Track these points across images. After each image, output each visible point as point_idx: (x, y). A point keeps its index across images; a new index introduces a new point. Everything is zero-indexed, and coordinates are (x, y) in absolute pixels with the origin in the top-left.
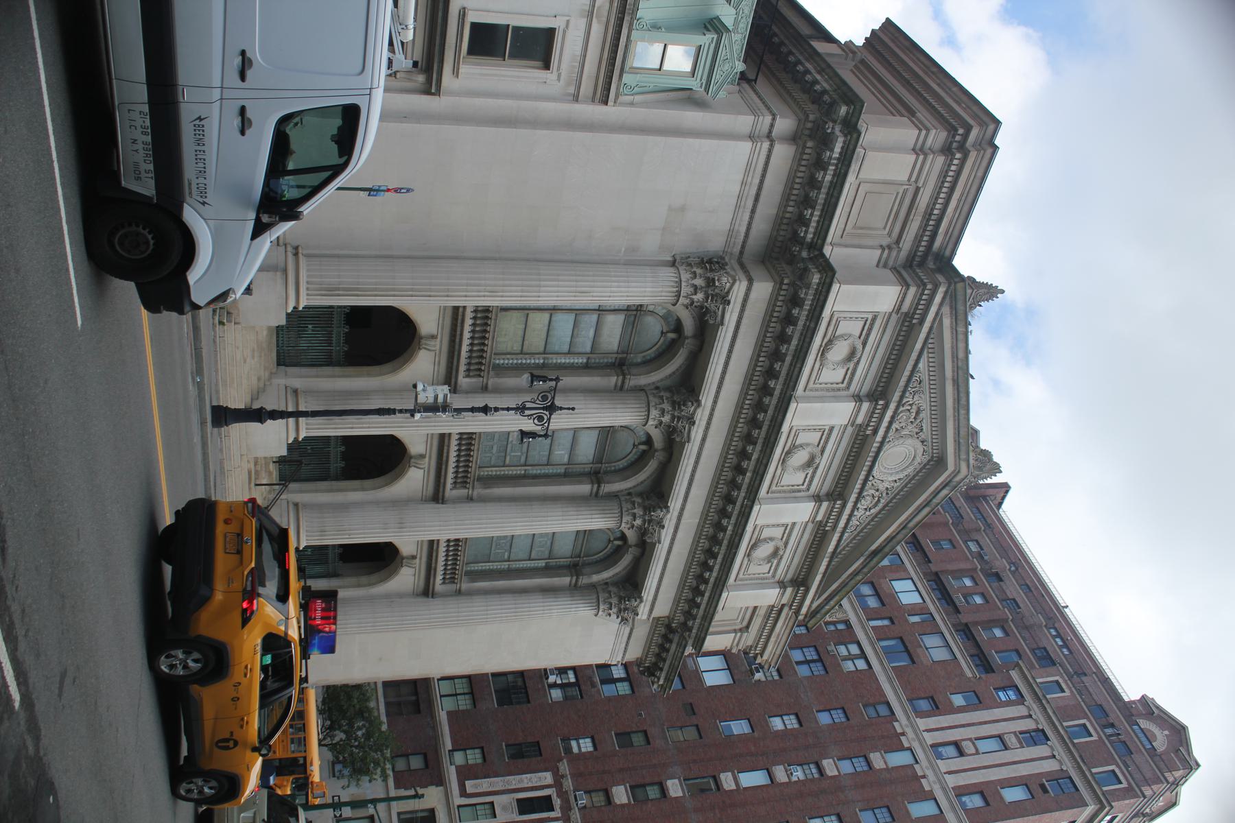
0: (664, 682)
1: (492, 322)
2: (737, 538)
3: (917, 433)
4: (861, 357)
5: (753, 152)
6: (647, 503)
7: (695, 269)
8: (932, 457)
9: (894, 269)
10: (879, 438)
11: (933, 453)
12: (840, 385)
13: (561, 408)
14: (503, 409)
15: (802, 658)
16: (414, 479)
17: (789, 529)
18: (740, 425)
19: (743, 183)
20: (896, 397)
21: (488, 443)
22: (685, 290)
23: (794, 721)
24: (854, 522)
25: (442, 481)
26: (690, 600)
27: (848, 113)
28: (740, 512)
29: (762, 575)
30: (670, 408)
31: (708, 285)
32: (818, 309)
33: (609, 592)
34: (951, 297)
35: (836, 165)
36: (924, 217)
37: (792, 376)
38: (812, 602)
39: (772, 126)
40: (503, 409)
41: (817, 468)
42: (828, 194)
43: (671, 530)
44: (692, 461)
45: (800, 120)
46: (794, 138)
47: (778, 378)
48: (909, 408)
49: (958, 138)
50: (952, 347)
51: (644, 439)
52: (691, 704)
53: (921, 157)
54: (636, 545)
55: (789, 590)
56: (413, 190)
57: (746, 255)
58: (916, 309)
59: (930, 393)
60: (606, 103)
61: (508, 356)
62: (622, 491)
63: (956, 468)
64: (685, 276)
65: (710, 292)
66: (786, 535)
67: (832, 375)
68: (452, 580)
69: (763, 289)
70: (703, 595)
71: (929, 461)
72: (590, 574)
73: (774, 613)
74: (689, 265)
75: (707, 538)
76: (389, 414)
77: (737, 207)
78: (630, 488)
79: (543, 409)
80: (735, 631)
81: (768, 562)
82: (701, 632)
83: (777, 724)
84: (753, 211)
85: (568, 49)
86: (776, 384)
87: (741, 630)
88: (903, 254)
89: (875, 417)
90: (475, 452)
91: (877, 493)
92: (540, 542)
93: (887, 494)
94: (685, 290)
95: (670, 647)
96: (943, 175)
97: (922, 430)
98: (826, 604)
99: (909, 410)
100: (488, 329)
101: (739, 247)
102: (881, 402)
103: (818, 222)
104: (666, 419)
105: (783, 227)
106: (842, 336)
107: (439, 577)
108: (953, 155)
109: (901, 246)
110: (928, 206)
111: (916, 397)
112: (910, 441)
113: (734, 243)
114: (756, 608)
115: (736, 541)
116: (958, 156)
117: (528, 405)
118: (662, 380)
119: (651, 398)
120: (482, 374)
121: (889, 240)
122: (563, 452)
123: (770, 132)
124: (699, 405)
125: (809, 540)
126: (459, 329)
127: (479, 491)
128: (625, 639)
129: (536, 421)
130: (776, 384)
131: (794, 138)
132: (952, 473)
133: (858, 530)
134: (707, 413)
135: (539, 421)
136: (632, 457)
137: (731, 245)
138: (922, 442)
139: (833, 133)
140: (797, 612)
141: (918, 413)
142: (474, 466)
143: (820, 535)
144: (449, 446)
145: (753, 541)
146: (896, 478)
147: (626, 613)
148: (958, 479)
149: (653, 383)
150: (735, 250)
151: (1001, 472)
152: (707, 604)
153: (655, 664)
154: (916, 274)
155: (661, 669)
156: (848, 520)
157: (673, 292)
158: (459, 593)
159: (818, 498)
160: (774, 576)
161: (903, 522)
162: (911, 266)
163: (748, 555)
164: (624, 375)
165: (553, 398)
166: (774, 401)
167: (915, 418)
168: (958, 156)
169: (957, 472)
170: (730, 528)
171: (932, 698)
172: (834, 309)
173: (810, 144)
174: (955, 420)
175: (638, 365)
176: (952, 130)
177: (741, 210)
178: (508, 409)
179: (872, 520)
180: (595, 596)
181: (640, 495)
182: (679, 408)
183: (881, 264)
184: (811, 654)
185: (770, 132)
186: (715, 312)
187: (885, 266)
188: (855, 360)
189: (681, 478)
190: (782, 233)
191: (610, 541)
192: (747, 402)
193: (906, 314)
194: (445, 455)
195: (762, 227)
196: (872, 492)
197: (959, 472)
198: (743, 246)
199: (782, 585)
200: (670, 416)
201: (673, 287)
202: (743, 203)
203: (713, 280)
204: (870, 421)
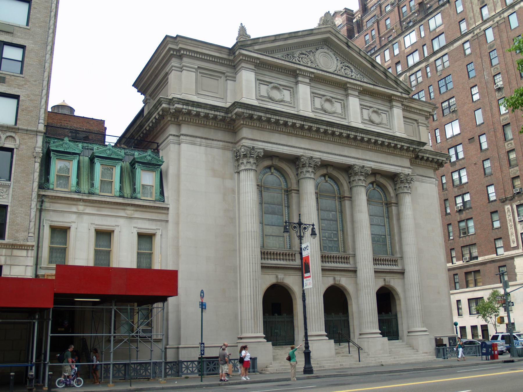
1: (269, 251)
3: (313, 53)
4: (278, 84)
6: (353, 174)
7: (240, 163)
8: (324, 44)
9: (236, 73)
10: (315, 71)
11: (322, 44)
12: (292, 91)
13: (300, 220)
15: (445, 87)
16: (344, 281)
17: (363, 107)
18: (312, 136)
19: (200, 145)
20: (296, 66)
21: (328, 249)
22: (249, 166)
23: (474, 88)
26: (400, 150)
27: (166, 103)
29: (388, 117)
30: (305, 168)
31: (246, 157)
33: (399, 188)
34: (245, 47)
39: (174, 135)
41: (332, 97)
43: (365, 162)
45: (171, 123)
46: (179, 125)
47: (287, 122)
48: (300, 58)
49: (175, 53)
50: (269, 43)
51: (323, 178)
52: (469, 140)
53: (184, 68)
54: (375, 177)
55: (394, 103)
56: (202, 290)
57: (233, 141)
58: (252, 62)
59: (293, 49)
60: (168, 208)
61: (285, 242)
62: (348, 186)
63: (328, 33)
64: (243, 167)
65: (249, 155)
66: (367, 108)
67: (286, 95)
68: (396, 261)
69: (245, 132)
70: (397, 145)
71: (326, 45)
72: (391, 197)
73: (406, 109)
74: (238, 165)
76: (305, 296)
78: (347, 182)
79: (300, 227)
80: (418, 126)
81: (380, 115)
83: (476, 97)
84: (213, 140)
85: (147, 227)
87: (418, 123)
88: (229, 70)
89: (304, 74)
91: (344, 68)
92: (376, 221)
93: (344, 63)
94: (249, 166)
95: (426, 157)
97: (311, 51)
99: (302, 58)
100: (272, 252)
101: (229, 144)
102: (298, 72)
104: (310, 170)
105: (219, 126)
106: (268, 93)
107: (395, 267)
108: (183, 54)
109: (225, 72)
111: (295, 56)
112: (317, 56)
113: (228, 146)
114: (404, 117)
116: (182, 52)
117: (298, 234)
118: (293, 173)
119: (301, 177)
120: (294, 254)
121: (223, 78)
122: (331, 215)
123: (177, 136)
127: (351, 252)
129: (306, 230)
131: (179, 125)
132: (331, 34)
133: (362, 74)
135: (306, 229)
136: (333, 183)
137: (229, 148)
138: (317, 50)
139: (175, 109)
140: (406, 99)
141: (303, 54)
143: (364, 92)
145: (369, 123)
146: (335, 60)
147: (408, 180)
149: (295, 176)
150: (231, 146)
151: (329, 12)
153: (436, 162)
154: (237, 63)
155: (438, 160)
157: (247, 173)
158: (402, 258)
159: (347, 95)
160: (387, 111)
161: (356, 54)
162: (234, 66)
163: (377, 125)
164: (291, 190)
165: (295, 223)
167: (306, 55)
168: (182, 52)
169: (329, 32)
171: (459, 22)
172: (255, 99)
173: (181, 118)
174: (305, 37)
175: (287, 185)
176: (172, 56)
177: (212, 145)
179: (357, 68)
180: (401, 194)
181: (349, 178)
182: (305, 164)
183: (234, 79)
184: (442, 83)
185: (177, 136)
186: (259, 152)
187: (235, 78)
188: (279, 86)
190: (221, 126)
191: (374, 189)
192: (300, 134)
193: (255, 66)
195: (220, 135)
196: (343, 70)
197: (330, 31)
198: (229, 142)
199: (391, 107)
200: (309, 168)
201: (247, 173)
203: (244, 155)
204: (307, 76)
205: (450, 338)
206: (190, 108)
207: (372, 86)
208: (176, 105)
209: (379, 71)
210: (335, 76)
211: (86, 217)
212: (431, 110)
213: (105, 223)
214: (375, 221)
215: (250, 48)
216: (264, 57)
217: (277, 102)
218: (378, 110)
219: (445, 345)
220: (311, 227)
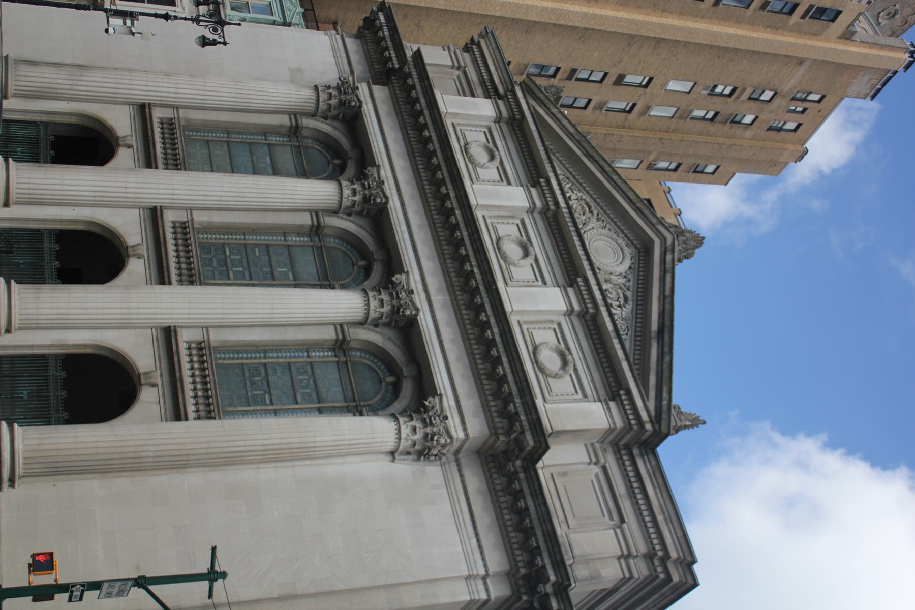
0: (556, 575)
2: (489, 276)
5: (331, 40)
13: (230, 24)
14: (181, 18)
16: (136, 267)
24: (619, 322)
25: (165, 264)
28: (474, 251)
30: (361, 189)
32: (423, 72)
34: (528, 93)
35: (387, 26)
36: (482, 86)
37: (437, 122)
40: (181, 18)
42: (392, 41)
44: (404, 227)
63: (661, 240)
75: (449, 243)
82: (531, 414)
86: (429, 132)
92: (302, 381)
96: (474, 61)
98: (661, 401)
103: (397, 57)
110: (479, 80)
115: (490, 279)
117: (201, 18)
122: (285, 270)
124: (378, 167)
125: (590, 346)
126: (149, 124)
130: (429, 132)
142: (195, 260)
144: (163, 226)
145: (531, 348)
148: (669, 242)
152: (513, 372)
156: (611, 315)
169: (663, 239)
170: (476, 271)
178: (185, 19)
189: (403, 247)
194: (161, 236)
197: (665, 239)
207: (610, 327)
212: (674, 555)
214: (301, 377)
215: (532, 102)
217: (466, 153)
220: (222, 40)
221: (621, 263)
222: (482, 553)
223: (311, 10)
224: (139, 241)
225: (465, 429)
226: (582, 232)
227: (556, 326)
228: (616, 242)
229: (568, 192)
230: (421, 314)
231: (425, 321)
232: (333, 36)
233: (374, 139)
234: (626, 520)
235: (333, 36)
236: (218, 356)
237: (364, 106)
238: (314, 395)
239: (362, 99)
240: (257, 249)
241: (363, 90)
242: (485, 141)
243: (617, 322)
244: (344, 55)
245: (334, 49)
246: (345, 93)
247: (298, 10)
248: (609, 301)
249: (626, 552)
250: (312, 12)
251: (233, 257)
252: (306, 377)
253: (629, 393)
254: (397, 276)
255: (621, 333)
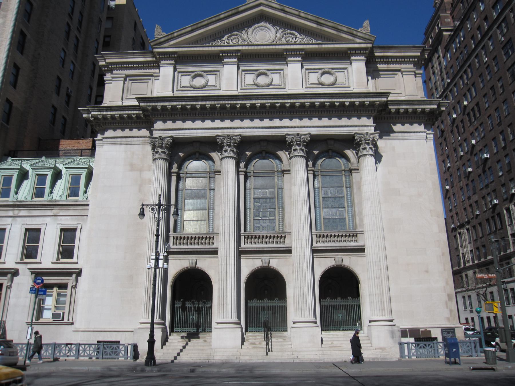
4: (201, 71)
5: (107, 144)
19: (121, 144)
38: (357, 43)
48: (230, 40)
69: (159, 125)
77: (115, 144)
90: (260, 234)
92: (331, 193)
113: (142, 141)
117: (156, 216)
128: (406, 134)
134: (231, 130)
145: (320, 86)
161: (296, 17)
166: (208, 103)
202: (129, 142)
205: (445, 331)
206: (105, 113)
207: (317, 46)
208: (93, 113)
209: (327, 28)
210: (274, 47)
211: (19, 219)
213: (33, 223)
214: (329, 193)
215: (166, 45)
216: (180, 49)
217: (198, 88)
218: (330, 70)
219: (436, 339)
221: (269, 29)
222: (417, 132)
223: (82, 152)
224: (260, 260)
225: (371, 126)
226: (250, 43)
227: (307, 71)
228: (256, 28)
229: (224, 43)
230: (311, 132)
231: (314, 131)
232: (104, 143)
233: (195, 134)
234: (400, 68)
235: (104, 143)
236: (351, 228)
237: (173, 135)
238: (339, 189)
239: (170, 135)
240: (255, 204)
241: (156, 134)
242: (189, 77)
243: (305, 42)
244: (141, 139)
245: (112, 144)
246: (162, 144)
247: (11, 161)
248: (293, 42)
249: (413, 73)
250: (83, 151)
251: (261, 216)
252: (329, 191)
253: (350, 49)
254: (287, 139)
255: (311, 42)
